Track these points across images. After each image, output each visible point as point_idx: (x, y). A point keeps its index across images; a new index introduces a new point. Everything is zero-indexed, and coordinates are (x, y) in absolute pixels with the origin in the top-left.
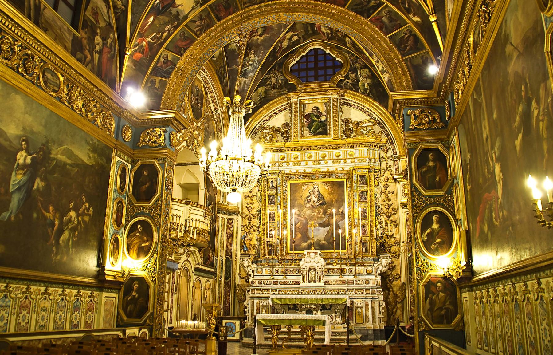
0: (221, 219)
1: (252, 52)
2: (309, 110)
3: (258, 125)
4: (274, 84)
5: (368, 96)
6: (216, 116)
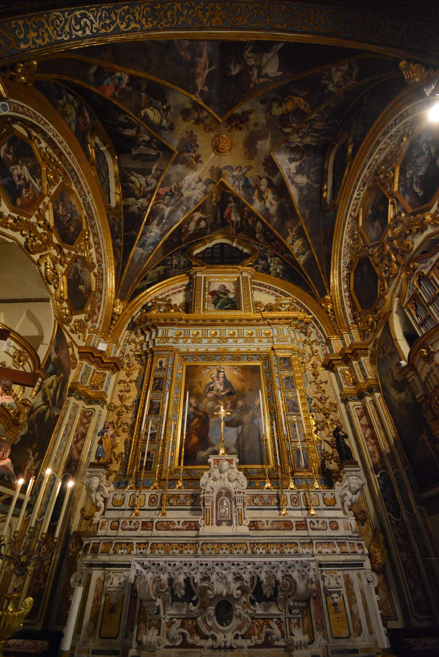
1: (155, 222)
2: (215, 287)
5: (282, 278)
6: (98, 272)
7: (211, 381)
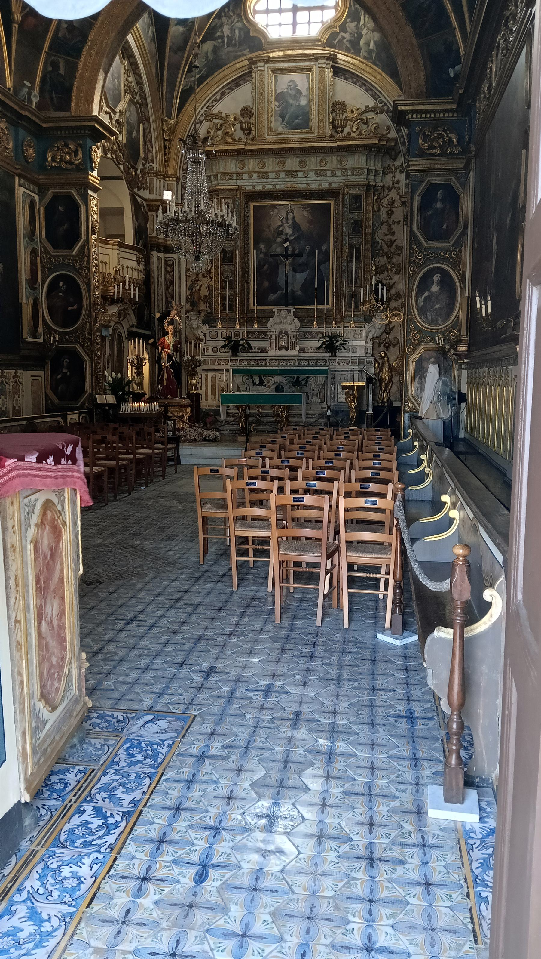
0: (156, 259)
3: (205, 109)
4: (228, 36)
7: (280, 223)
